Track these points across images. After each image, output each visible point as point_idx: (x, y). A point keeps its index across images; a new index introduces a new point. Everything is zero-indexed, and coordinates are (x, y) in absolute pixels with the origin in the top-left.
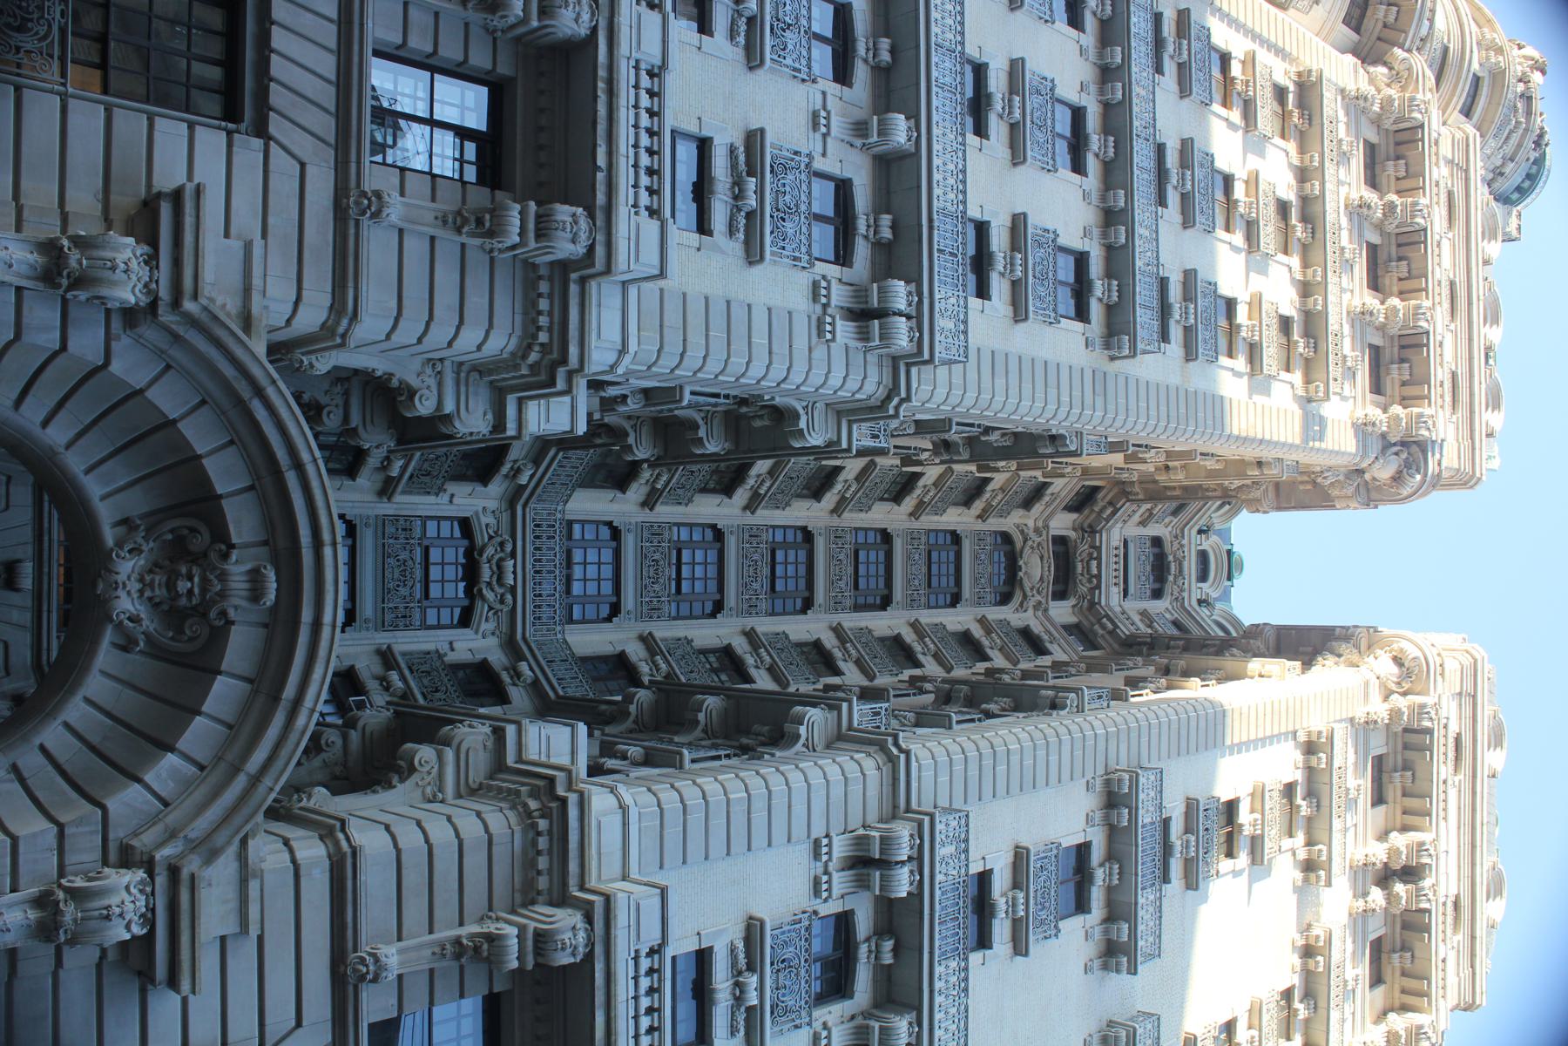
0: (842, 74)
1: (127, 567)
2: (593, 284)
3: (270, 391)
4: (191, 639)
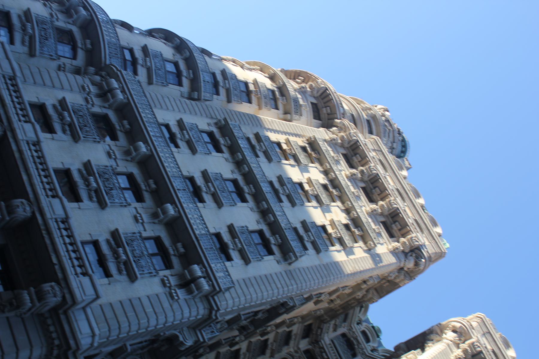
0: (139, 198)
2: (70, 312)
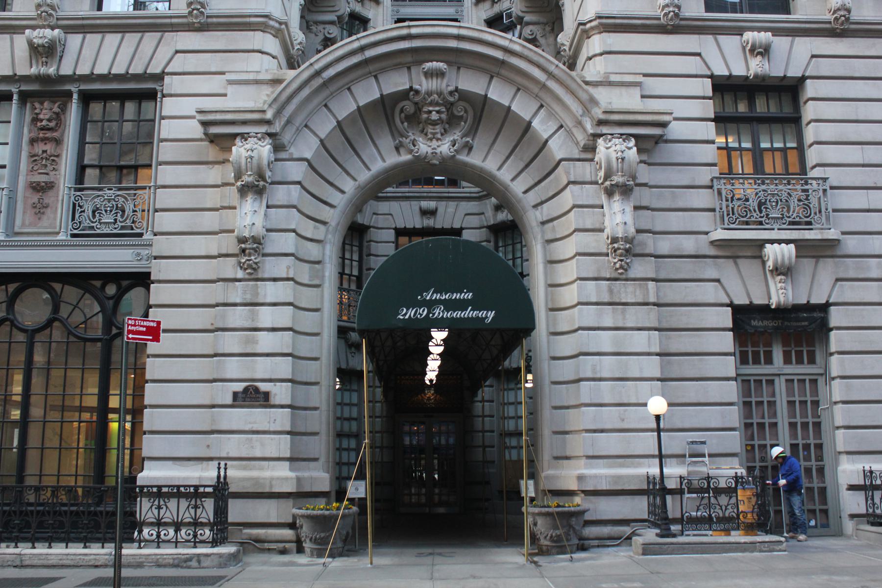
1: (424, 147)
3: (317, 67)
4: (466, 111)
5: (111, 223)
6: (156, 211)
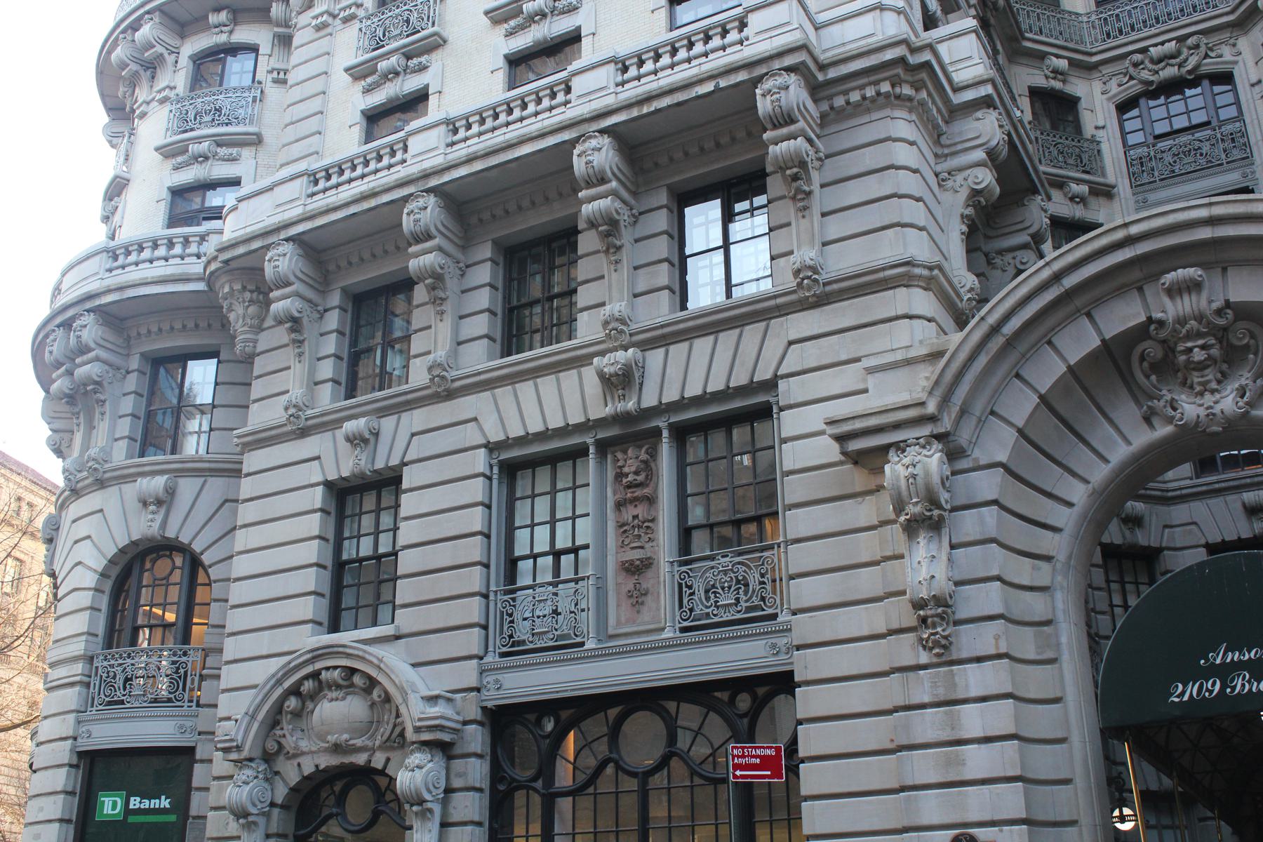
1: (1191, 409)
2: (823, 58)
3: (992, 320)
4: (1252, 336)
5: (730, 605)
6: (792, 578)
